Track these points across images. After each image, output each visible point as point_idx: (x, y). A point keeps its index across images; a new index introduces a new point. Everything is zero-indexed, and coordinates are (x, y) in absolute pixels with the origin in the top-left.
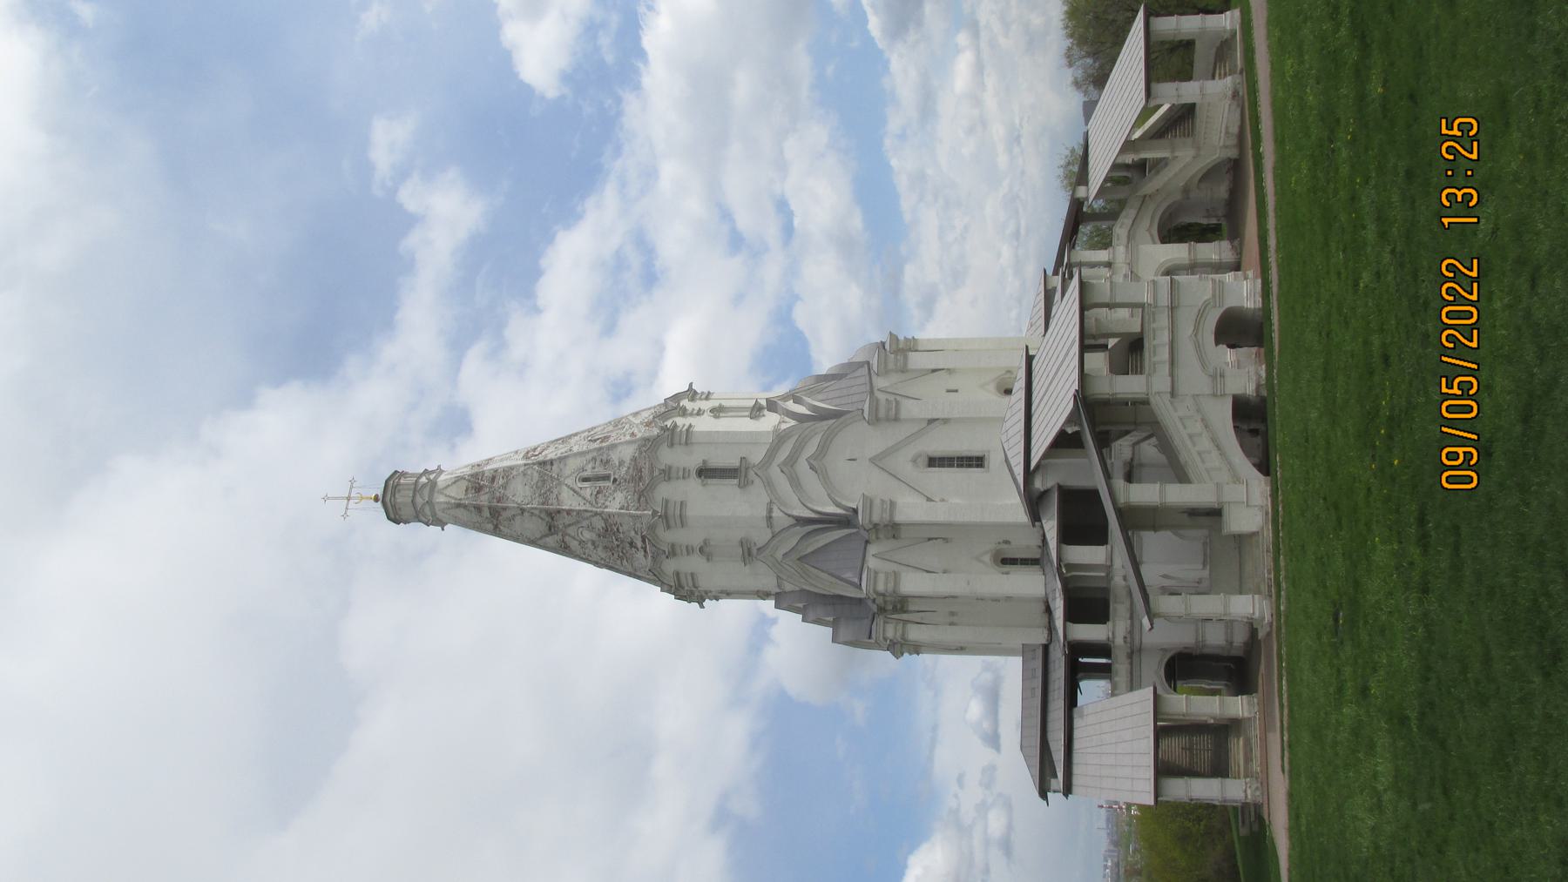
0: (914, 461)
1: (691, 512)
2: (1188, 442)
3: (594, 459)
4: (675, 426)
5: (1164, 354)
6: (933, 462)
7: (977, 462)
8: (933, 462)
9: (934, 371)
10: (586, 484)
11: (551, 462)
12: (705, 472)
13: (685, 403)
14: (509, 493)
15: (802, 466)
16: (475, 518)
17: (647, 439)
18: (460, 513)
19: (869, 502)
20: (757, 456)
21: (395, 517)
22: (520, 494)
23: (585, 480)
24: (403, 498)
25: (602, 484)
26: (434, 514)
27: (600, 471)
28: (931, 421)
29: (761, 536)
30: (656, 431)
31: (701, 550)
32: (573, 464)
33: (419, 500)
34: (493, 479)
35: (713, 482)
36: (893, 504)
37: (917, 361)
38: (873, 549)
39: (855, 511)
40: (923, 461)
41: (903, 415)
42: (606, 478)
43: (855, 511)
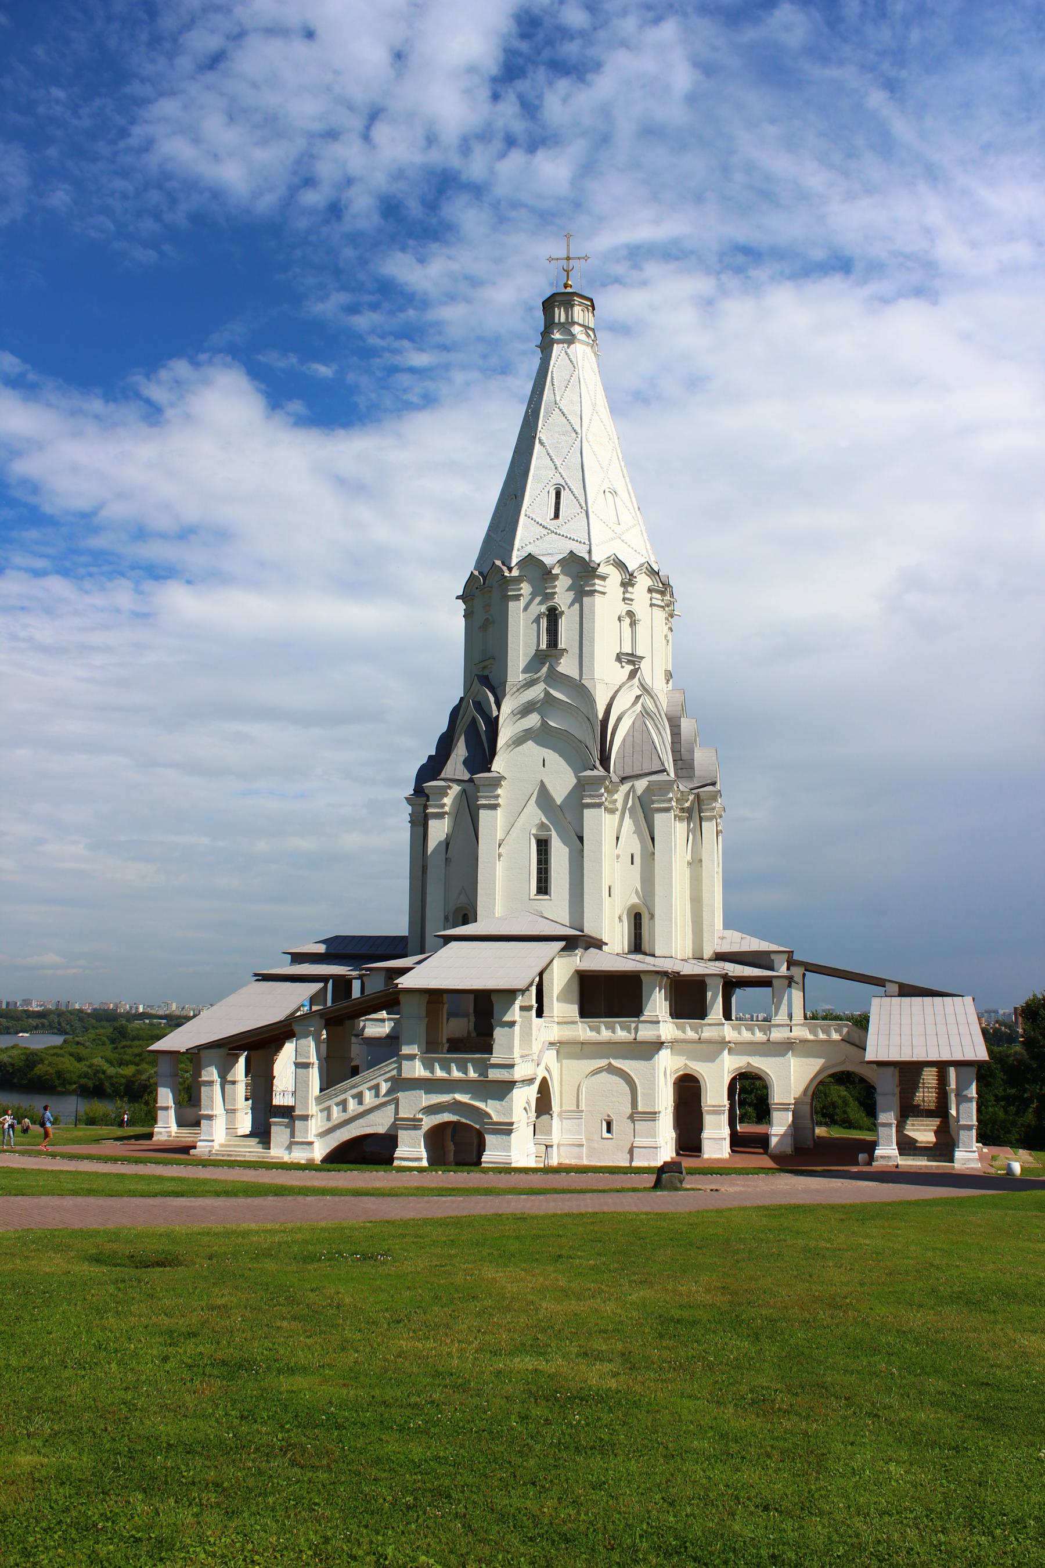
2: (355, 1091)
5: (440, 1073)
7: (543, 887)
9: (653, 839)
12: (553, 616)
13: (643, 582)
19: (497, 782)
20: (567, 666)
28: (581, 839)
35: (544, 623)
36: (494, 807)
39: (489, 770)
40: (543, 834)
41: (587, 812)
43: (489, 770)
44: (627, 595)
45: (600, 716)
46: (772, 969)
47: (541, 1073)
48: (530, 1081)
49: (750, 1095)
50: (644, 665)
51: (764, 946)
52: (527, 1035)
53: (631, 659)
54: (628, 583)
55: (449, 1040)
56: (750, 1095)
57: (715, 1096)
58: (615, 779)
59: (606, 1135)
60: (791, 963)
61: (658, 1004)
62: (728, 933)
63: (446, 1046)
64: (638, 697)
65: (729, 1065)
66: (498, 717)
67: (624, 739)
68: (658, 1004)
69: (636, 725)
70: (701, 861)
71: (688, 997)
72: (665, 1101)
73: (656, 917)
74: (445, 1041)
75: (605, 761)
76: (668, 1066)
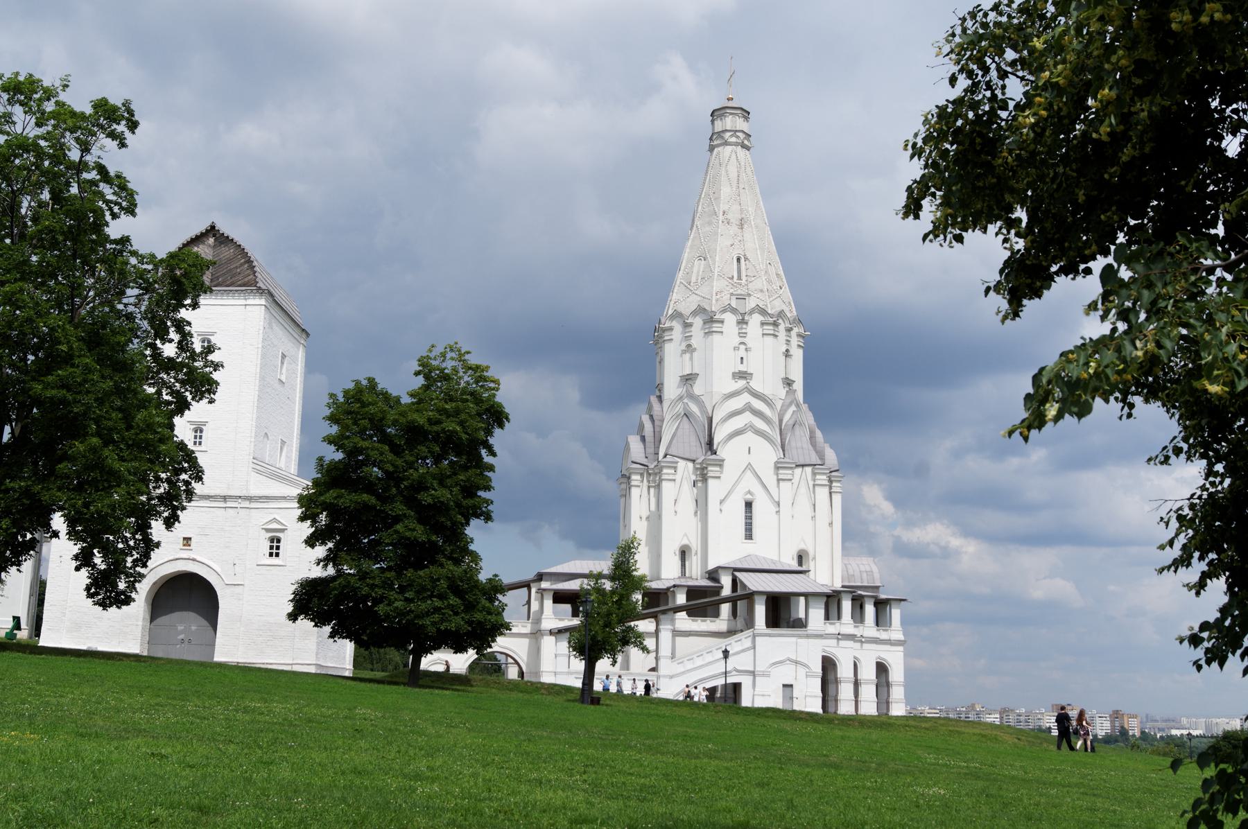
0: (749, 492)
1: (716, 337)
6: (749, 505)
7: (749, 535)
8: (749, 505)
15: (747, 418)
20: (755, 384)
21: (716, 114)
24: (730, 122)
26: (718, 146)
29: (698, 389)
31: (689, 346)
33: (728, 134)
37: (822, 493)
38: (690, 465)
40: (749, 497)
41: (782, 483)
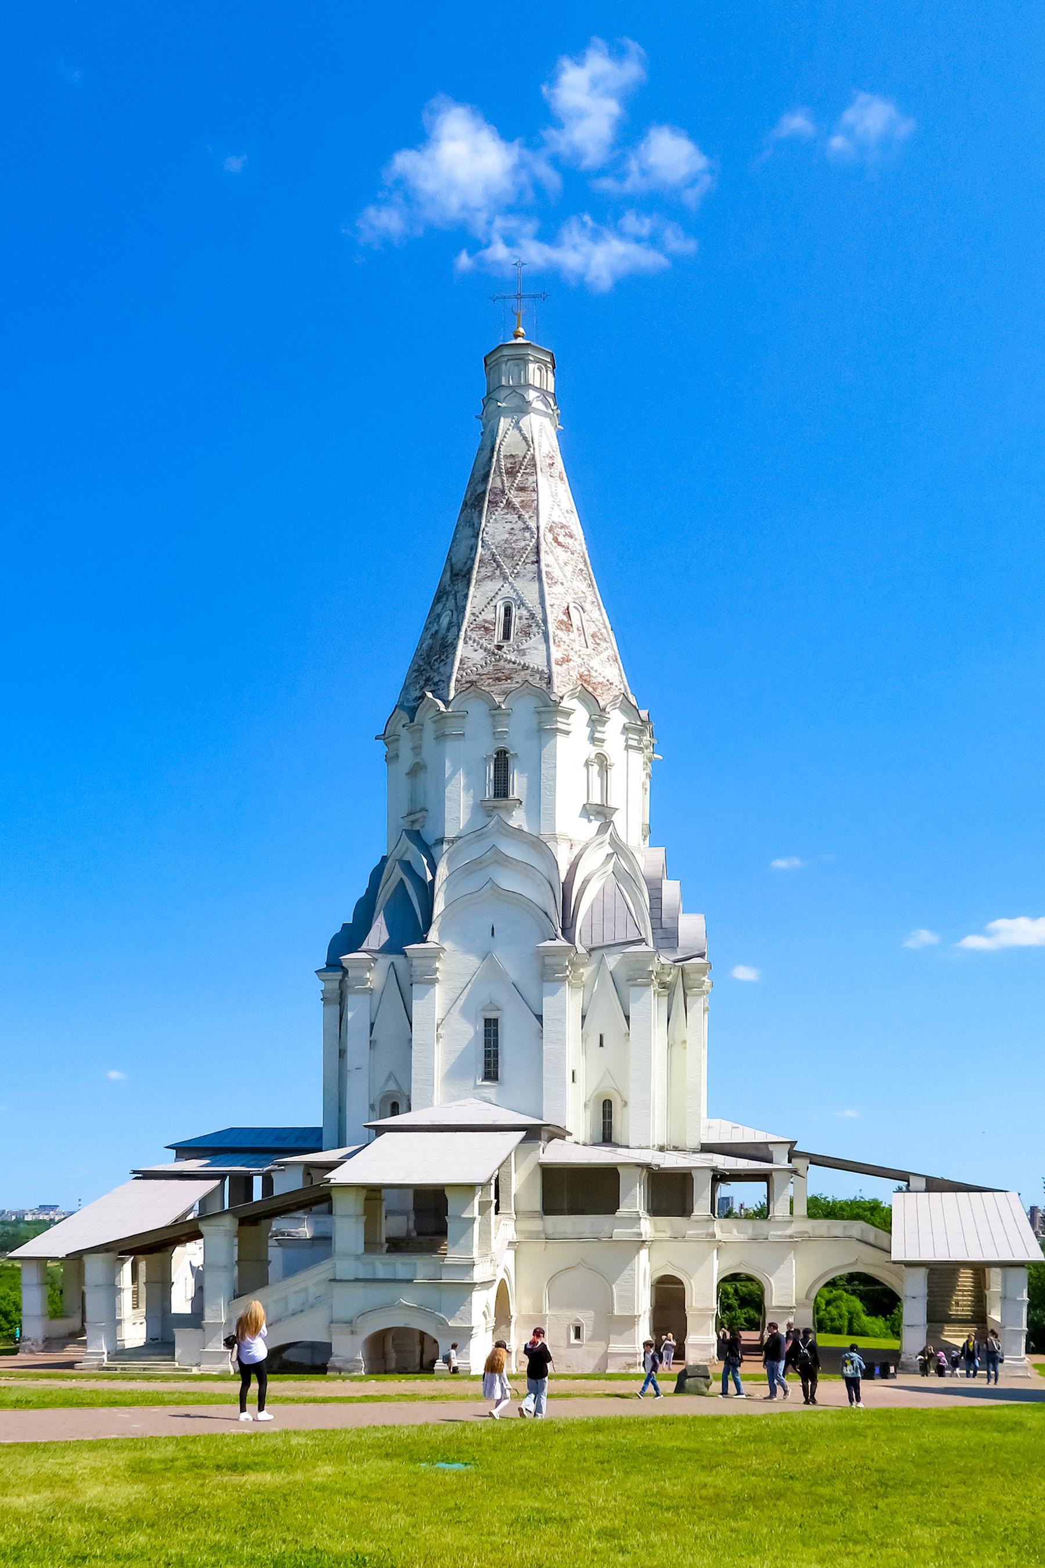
3: (532, 616)
4: (568, 714)
10: (501, 611)
11: (538, 562)
14: (499, 512)
16: (479, 475)
17: (550, 681)
18: (486, 452)
22: (495, 528)
23: (508, 611)
25: (499, 630)
27: (516, 625)
28: (540, 1018)
30: (561, 687)
32: (529, 592)
34: (522, 489)
42: (506, 636)
44: (597, 735)
45: (563, 878)
46: (770, 1161)
47: (501, 1275)
48: (487, 1284)
49: (742, 1298)
50: (617, 818)
51: (761, 1137)
52: (485, 1232)
53: (600, 813)
54: (598, 718)
55: (388, 1240)
56: (742, 1298)
57: (702, 1300)
58: (581, 950)
59: (573, 1341)
60: (792, 1155)
61: (634, 1198)
62: (716, 1122)
63: (386, 1246)
64: (609, 856)
65: (715, 1268)
66: (433, 881)
67: (592, 906)
68: (634, 1198)
69: (607, 889)
70: (684, 1042)
71: (670, 1192)
72: (644, 1304)
73: (631, 1104)
74: (384, 1240)
75: (568, 929)
76: (644, 1270)
